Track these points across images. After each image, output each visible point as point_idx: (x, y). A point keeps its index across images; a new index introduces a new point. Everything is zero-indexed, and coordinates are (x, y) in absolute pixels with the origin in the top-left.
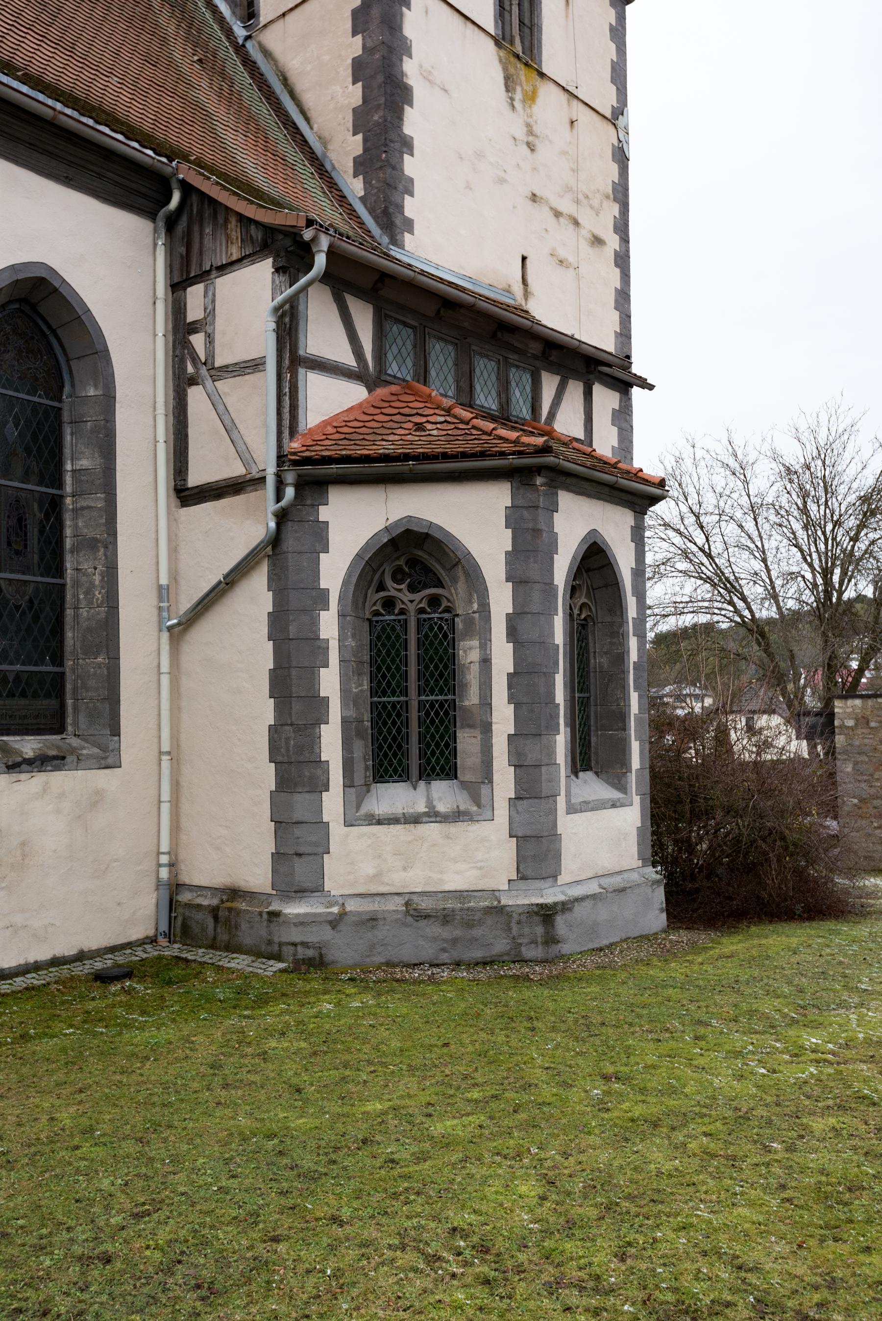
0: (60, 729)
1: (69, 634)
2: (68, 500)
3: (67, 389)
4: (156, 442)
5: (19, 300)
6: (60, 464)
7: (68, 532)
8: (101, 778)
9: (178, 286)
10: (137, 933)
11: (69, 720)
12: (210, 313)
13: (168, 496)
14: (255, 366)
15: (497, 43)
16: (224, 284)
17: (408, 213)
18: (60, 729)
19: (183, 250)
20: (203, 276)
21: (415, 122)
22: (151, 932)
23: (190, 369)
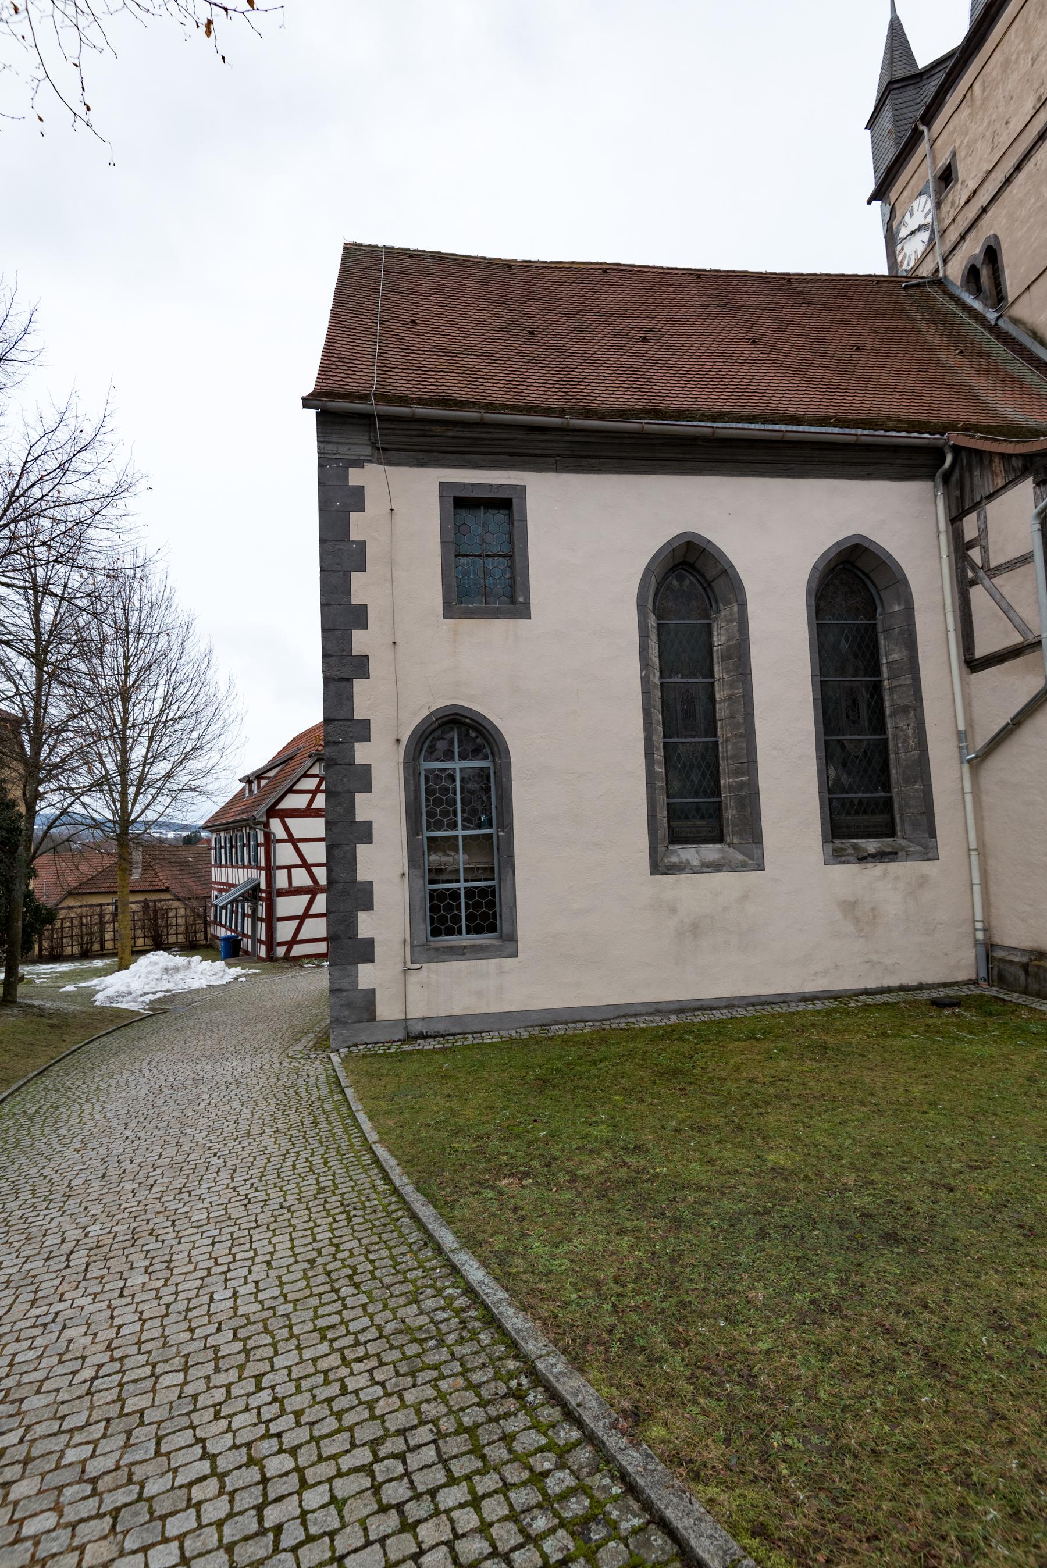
0: (892, 834)
1: (893, 771)
2: (886, 683)
3: (879, 610)
4: (947, 631)
5: (843, 563)
6: (878, 660)
7: (887, 704)
9: (955, 519)
10: (962, 976)
11: (898, 828)
12: (983, 531)
13: (960, 668)
14: (1026, 559)
16: (992, 508)
18: (892, 834)
19: (958, 493)
20: (976, 506)
22: (974, 977)
23: (970, 574)
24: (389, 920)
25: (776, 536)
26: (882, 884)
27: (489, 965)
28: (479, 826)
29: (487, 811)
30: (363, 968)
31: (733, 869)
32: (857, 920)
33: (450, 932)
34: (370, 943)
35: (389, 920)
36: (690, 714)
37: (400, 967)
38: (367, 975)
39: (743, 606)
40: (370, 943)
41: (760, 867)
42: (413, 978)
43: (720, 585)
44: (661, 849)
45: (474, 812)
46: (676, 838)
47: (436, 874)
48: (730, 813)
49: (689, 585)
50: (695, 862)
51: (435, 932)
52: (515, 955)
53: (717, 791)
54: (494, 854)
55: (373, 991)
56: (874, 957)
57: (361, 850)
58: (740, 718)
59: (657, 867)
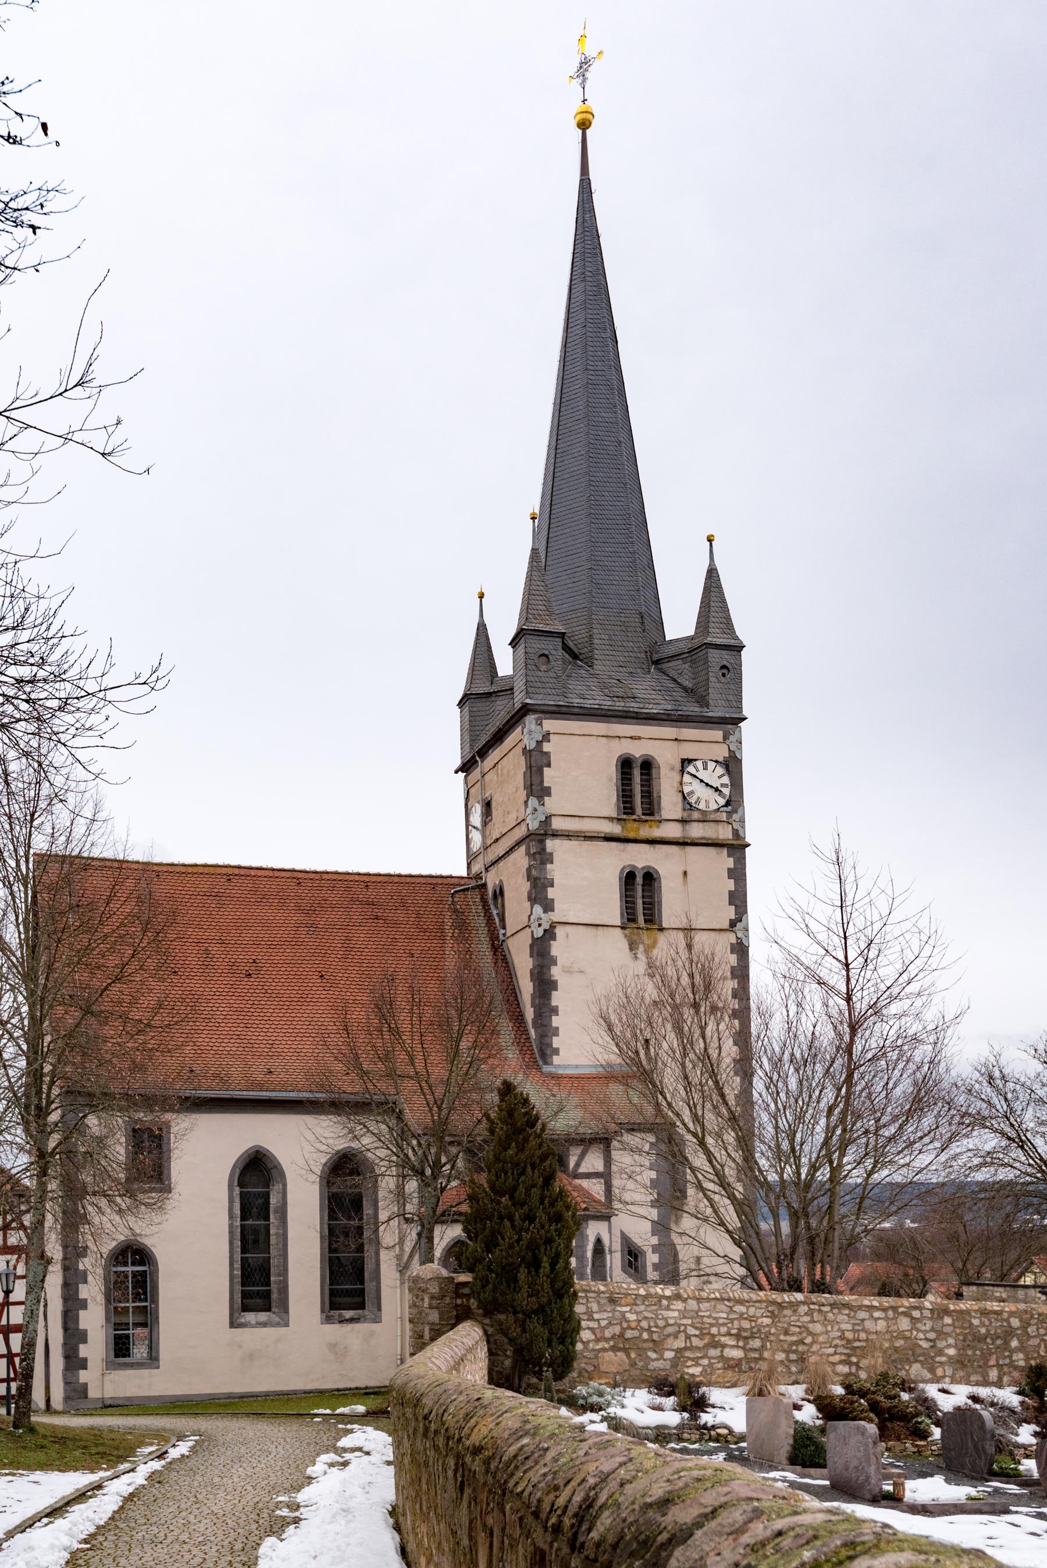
8: (374, 1326)
15: (623, 928)
17: (555, 1046)
21: (557, 999)
24: (95, 1348)
25: (302, 1148)
26: (351, 1335)
27: (145, 1372)
28: (140, 1300)
29: (145, 1293)
30: (82, 1372)
31: (272, 1326)
32: (336, 1353)
33: (124, 1356)
34: (86, 1360)
35: (95, 1348)
36: (256, 1241)
37: (100, 1372)
38: (83, 1376)
39: (285, 1186)
40: (86, 1360)
41: (287, 1325)
42: (107, 1378)
43: (274, 1172)
44: (236, 1315)
46: (245, 1308)
47: (117, 1326)
48: (274, 1296)
49: (256, 1173)
50: (253, 1322)
51: (117, 1356)
52: (158, 1367)
53: (268, 1283)
54: (148, 1318)
55: (86, 1384)
56: (344, 1373)
57: (81, 1313)
58: (281, 1246)
59: (232, 1325)
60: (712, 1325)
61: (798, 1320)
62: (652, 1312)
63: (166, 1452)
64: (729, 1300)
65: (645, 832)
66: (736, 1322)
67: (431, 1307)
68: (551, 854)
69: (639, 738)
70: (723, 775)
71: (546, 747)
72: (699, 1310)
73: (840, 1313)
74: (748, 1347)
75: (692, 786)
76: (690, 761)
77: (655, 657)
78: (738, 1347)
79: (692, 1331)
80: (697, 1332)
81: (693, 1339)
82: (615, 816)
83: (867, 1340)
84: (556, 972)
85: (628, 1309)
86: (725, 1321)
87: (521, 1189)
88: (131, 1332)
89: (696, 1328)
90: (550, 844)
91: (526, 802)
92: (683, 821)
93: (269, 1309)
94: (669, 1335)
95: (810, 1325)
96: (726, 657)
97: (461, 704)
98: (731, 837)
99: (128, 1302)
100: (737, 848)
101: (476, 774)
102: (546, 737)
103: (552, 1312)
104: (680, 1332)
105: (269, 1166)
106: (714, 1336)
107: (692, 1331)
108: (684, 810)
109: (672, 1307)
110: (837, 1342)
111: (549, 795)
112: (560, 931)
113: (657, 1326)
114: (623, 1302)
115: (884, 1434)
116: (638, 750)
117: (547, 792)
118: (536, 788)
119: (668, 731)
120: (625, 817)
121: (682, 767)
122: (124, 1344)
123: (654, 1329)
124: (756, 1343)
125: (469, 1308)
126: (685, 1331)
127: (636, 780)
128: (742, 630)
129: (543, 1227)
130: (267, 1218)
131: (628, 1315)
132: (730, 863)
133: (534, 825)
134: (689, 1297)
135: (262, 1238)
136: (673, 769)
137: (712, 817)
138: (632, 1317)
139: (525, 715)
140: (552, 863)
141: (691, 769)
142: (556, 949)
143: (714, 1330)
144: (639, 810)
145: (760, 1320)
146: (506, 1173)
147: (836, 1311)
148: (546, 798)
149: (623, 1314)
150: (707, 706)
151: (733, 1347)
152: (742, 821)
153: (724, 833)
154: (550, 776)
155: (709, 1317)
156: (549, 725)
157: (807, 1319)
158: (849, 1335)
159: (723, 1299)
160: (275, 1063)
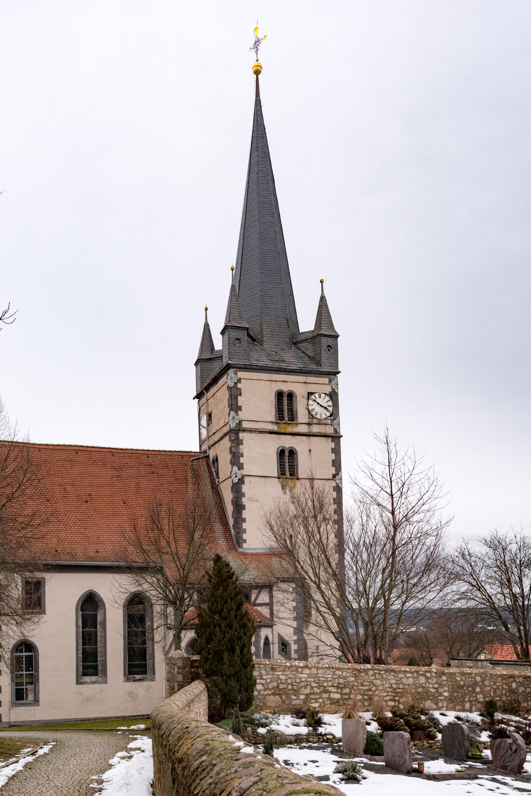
0: (146, 674)
8: (152, 683)
15: (278, 478)
17: (244, 538)
18: (146, 674)
21: (245, 514)
26: (139, 688)
27: (32, 708)
28: (30, 671)
29: (32, 667)
31: (99, 683)
32: (132, 697)
33: (21, 700)
36: (90, 639)
37: (8, 708)
39: (105, 610)
41: (106, 683)
42: (12, 711)
43: (99, 603)
44: (79, 678)
45: (28, 667)
46: (84, 674)
47: (17, 684)
48: (100, 668)
49: (90, 604)
50: (89, 682)
51: (17, 700)
52: (39, 705)
53: (96, 661)
54: (33, 680)
56: (136, 707)
58: (103, 642)
59: (78, 683)
60: (324, 681)
61: (368, 679)
62: (293, 675)
63: (37, 751)
64: (333, 668)
65: (289, 429)
66: (336, 680)
67: (178, 673)
68: (242, 440)
69: (287, 382)
70: (329, 401)
71: (239, 386)
72: (318, 673)
73: (390, 674)
74: (343, 692)
75: (313, 406)
76: (312, 394)
77: (294, 341)
78: (337, 692)
79: (314, 685)
80: (317, 685)
81: (314, 688)
82: (274, 421)
83: (403, 689)
84: (244, 500)
85: (281, 673)
86: (331, 679)
87: (225, 611)
88: (25, 687)
89: (316, 683)
90: (242, 435)
91: (229, 414)
92: (309, 424)
93: (97, 675)
94: (302, 687)
95: (375, 681)
96: (330, 341)
97: (196, 364)
98: (333, 432)
99: (22, 670)
100: (336, 438)
101: (204, 400)
102: (239, 381)
103: (241, 675)
104: (308, 685)
105: (97, 600)
106: (325, 687)
107: (314, 685)
108: (309, 418)
109: (303, 672)
110: (388, 689)
111: (241, 410)
112: (246, 480)
113: (296, 682)
114: (278, 669)
115: (413, 737)
116: (286, 388)
117: (240, 408)
118: (234, 406)
119: (301, 378)
120: (279, 421)
121: (308, 396)
122: (21, 693)
123: (294, 684)
124: (347, 691)
125: (198, 673)
126: (310, 685)
127: (285, 403)
128: (338, 328)
129: (236, 631)
130: (96, 627)
131: (281, 676)
132: (333, 445)
133: (233, 425)
134: (312, 667)
135: (93, 638)
136: (303, 397)
137: (323, 422)
138: (283, 677)
139: (228, 369)
140: (242, 445)
141: (313, 397)
142: (245, 488)
143: (325, 684)
144: (286, 418)
145: (349, 679)
146: (217, 603)
147: (387, 674)
148: (239, 412)
149: (278, 676)
150: (321, 366)
151: (335, 692)
152: (339, 424)
153: (330, 430)
154: (241, 400)
155: (323, 677)
156: (241, 374)
157: (373, 678)
158: (394, 686)
159: (330, 668)
160: (100, 547)
